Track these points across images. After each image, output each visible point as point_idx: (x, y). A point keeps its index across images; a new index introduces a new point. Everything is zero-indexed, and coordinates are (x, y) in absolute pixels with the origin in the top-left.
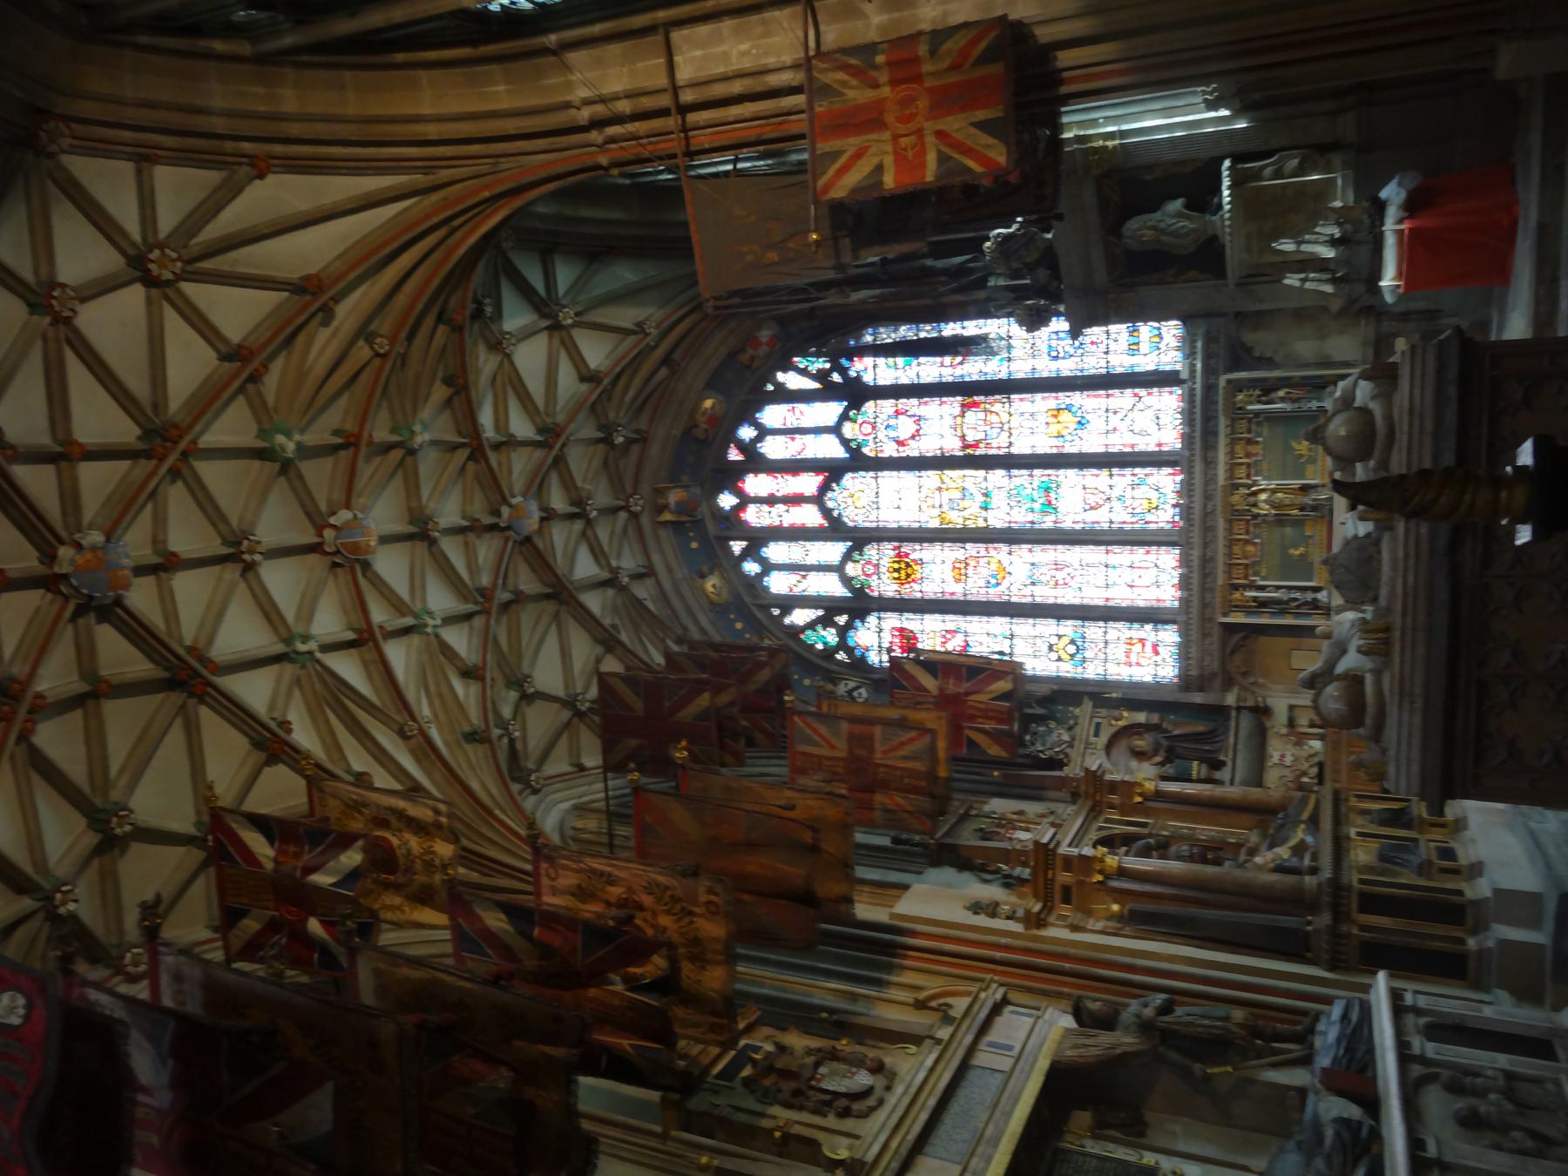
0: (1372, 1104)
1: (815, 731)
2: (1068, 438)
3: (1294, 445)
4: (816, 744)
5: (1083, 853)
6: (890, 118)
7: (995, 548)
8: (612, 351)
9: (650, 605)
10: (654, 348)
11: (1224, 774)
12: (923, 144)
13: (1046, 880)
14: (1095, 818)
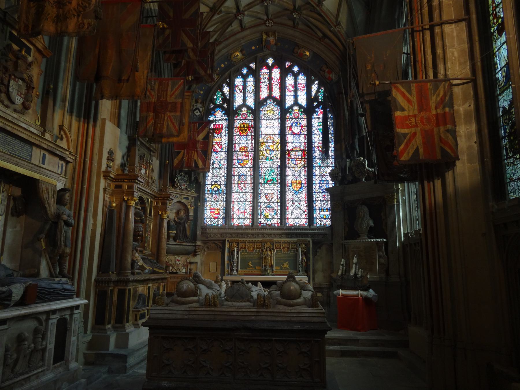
0: (22, 303)
1: (178, 88)
2: (291, 188)
3: (287, 263)
4: (172, 90)
5: (135, 193)
6: (423, 114)
7: (252, 162)
8: (329, 11)
9: (229, 30)
10: (330, 31)
11: (171, 241)
12: (411, 127)
13: (124, 179)
14: (152, 198)
